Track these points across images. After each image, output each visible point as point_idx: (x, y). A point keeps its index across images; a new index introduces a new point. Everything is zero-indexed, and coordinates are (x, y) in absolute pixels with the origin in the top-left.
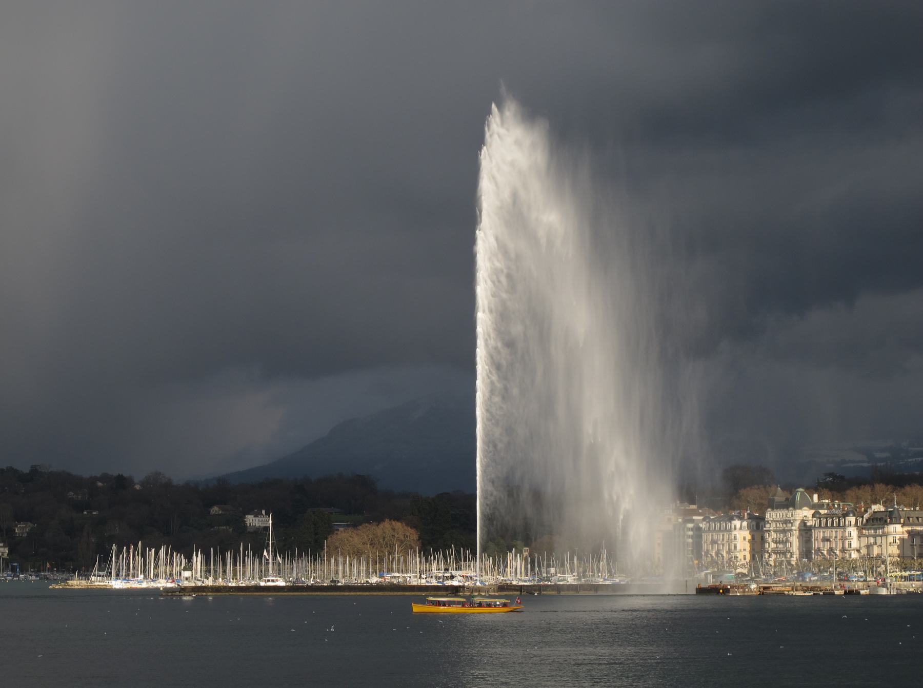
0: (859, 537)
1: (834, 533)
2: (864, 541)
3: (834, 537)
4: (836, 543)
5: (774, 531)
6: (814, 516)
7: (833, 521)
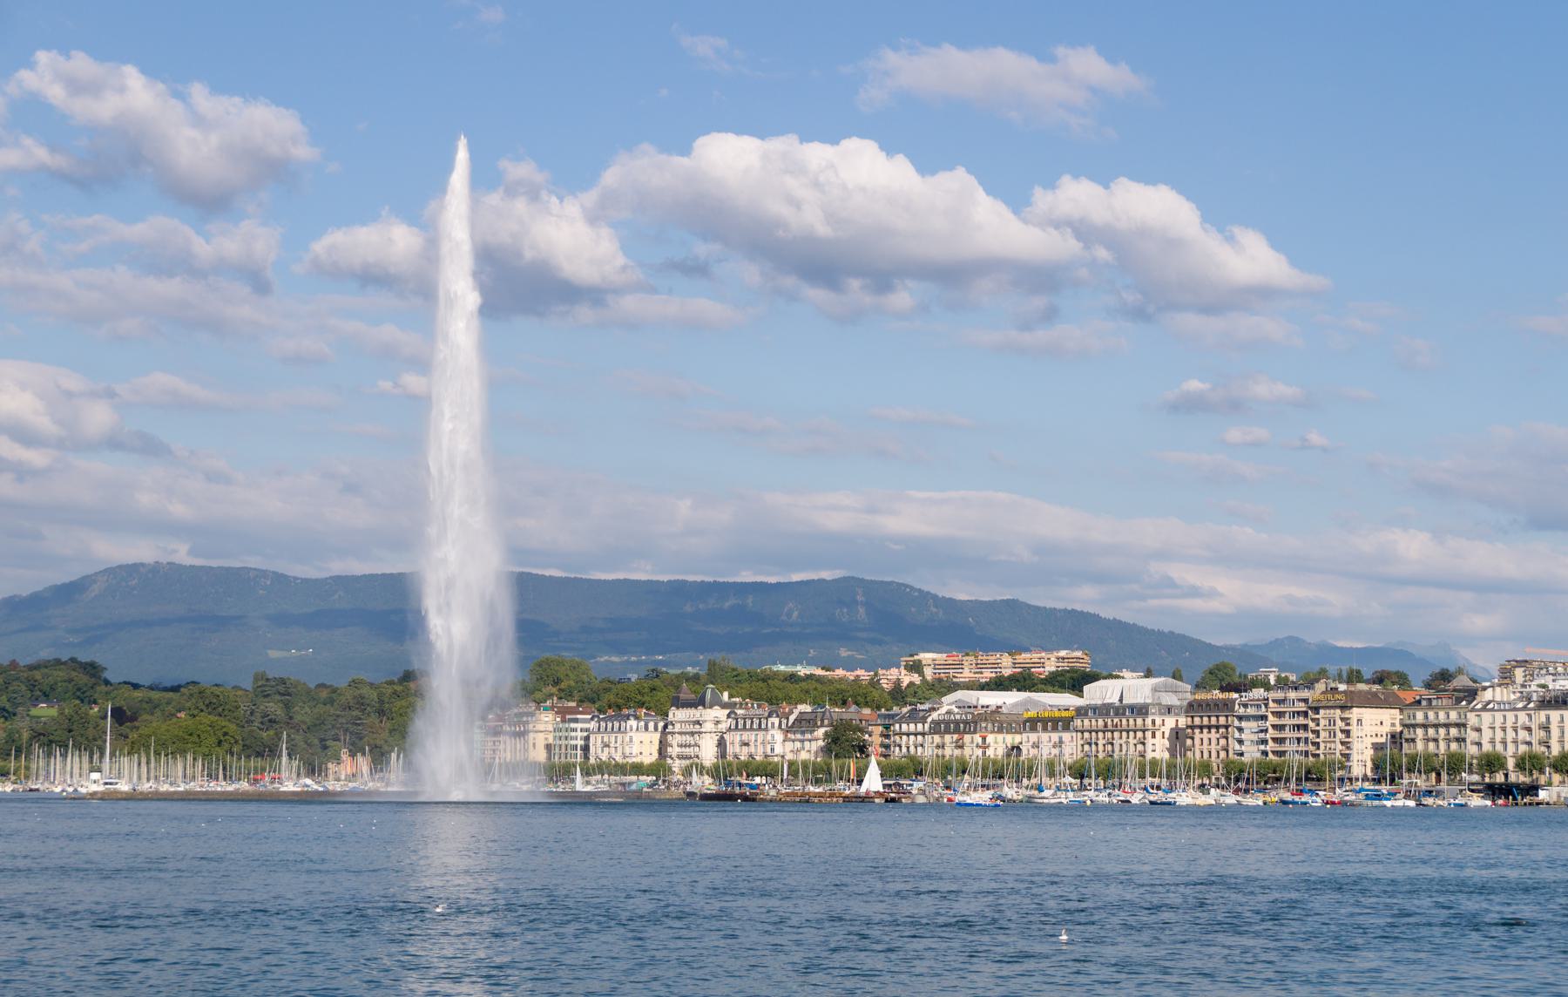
0: (784, 741)
2: (789, 745)
3: (753, 741)
5: (679, 733)
6: (729, 716)
7: (752, 722)
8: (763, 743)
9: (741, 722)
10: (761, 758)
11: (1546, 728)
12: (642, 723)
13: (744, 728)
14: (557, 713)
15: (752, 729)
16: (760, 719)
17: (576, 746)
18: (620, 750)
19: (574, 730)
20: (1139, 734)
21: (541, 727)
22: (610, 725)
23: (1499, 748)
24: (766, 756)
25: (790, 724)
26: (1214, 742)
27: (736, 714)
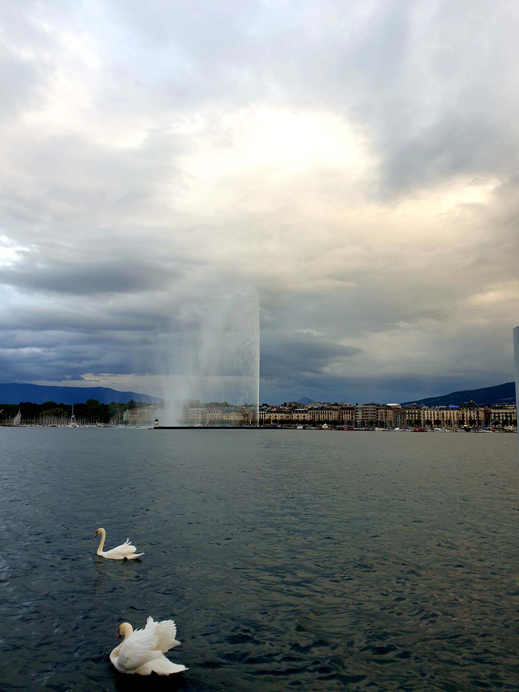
11: (443, 414)
13: (212, 412)
20: (327, 415)
23: (429, 419)
26: (348, 417)
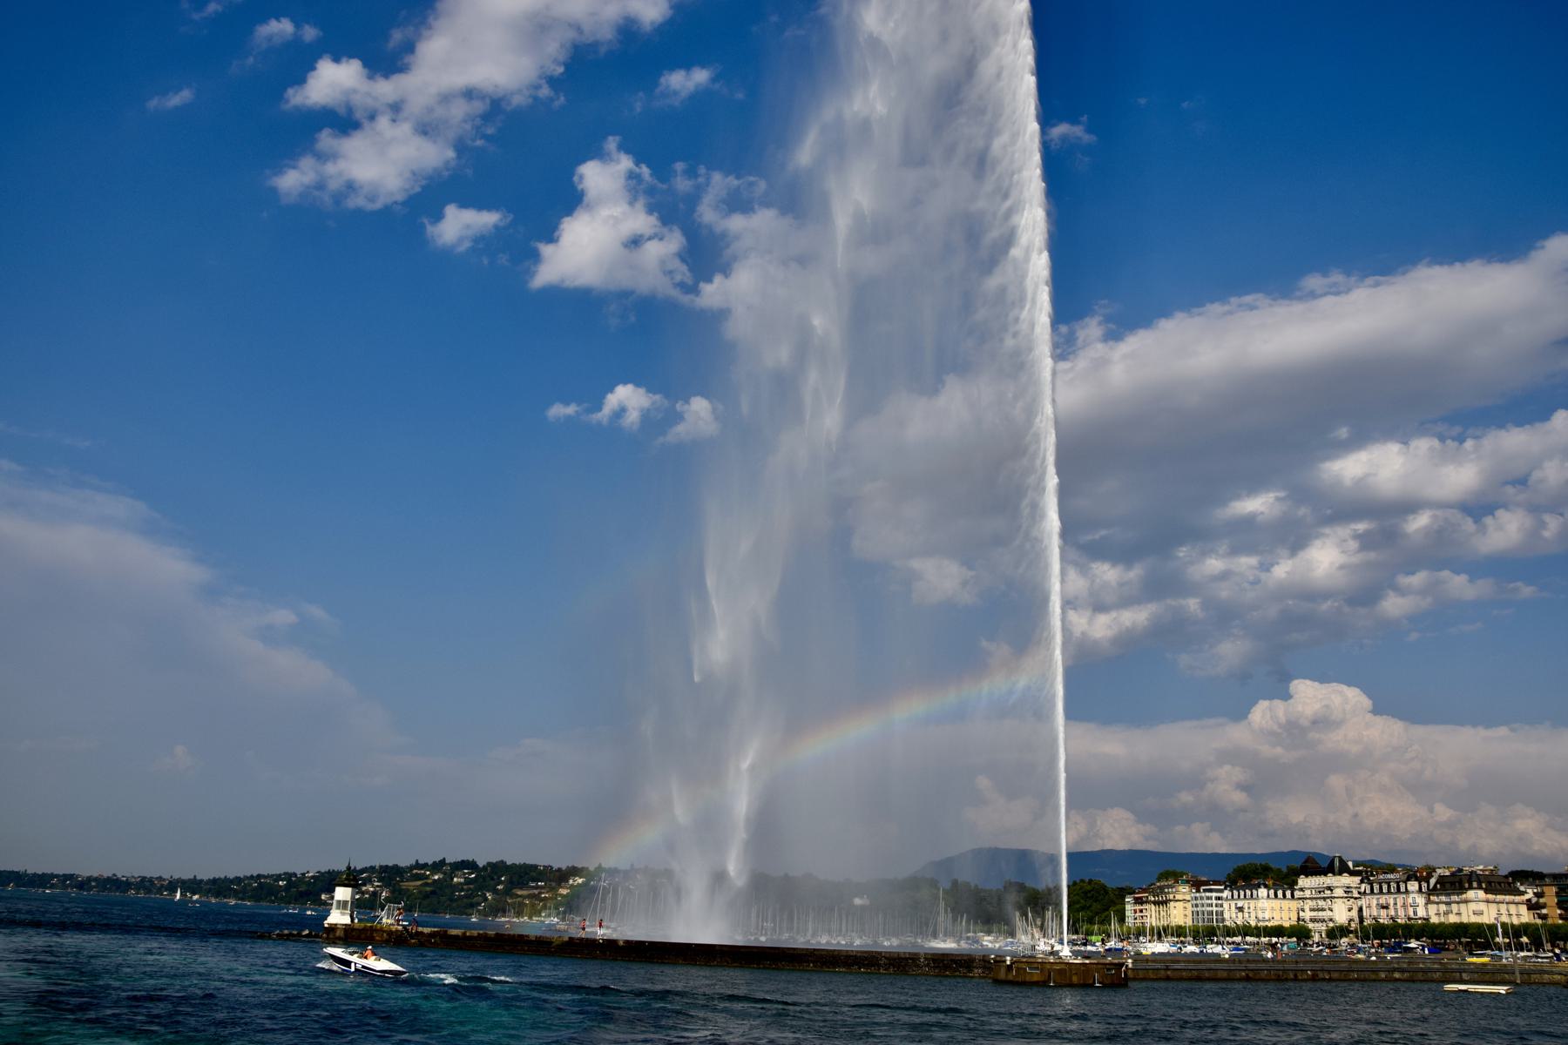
0: (1426, 904)
1: (1392, 899)
2: (1433, 909)
3: (1392, 905)
4: (1396, 910)
6: (1362, 882)
8: (1404, 906)
9: (1376, 887)
10: (1403, 922)
12: (1272, 892)
13: (1381, 892)
14: (1192, 885)
15: (1389, 892)
16: (1398, 883)
17: (1212, 912)
18: (1253, 915)
19: (1208, 898)
21: (1178, 897)
22: (1242, 893)
24: (1410, 919)
25: (1431, 887)
27: (1369, 880)
